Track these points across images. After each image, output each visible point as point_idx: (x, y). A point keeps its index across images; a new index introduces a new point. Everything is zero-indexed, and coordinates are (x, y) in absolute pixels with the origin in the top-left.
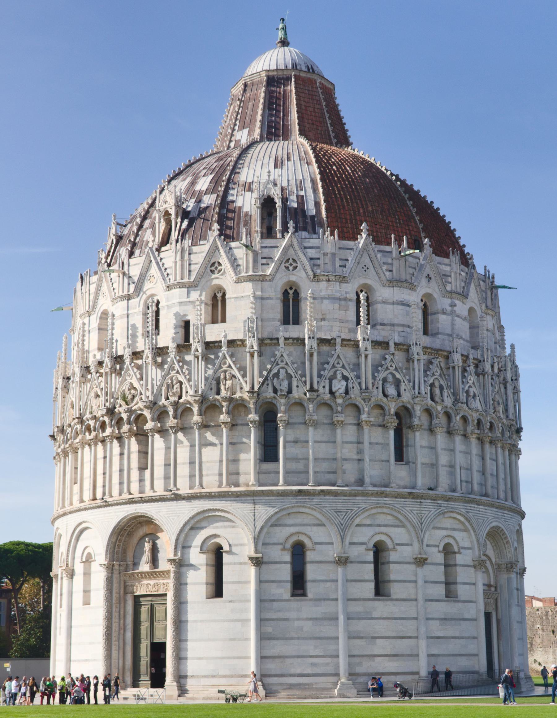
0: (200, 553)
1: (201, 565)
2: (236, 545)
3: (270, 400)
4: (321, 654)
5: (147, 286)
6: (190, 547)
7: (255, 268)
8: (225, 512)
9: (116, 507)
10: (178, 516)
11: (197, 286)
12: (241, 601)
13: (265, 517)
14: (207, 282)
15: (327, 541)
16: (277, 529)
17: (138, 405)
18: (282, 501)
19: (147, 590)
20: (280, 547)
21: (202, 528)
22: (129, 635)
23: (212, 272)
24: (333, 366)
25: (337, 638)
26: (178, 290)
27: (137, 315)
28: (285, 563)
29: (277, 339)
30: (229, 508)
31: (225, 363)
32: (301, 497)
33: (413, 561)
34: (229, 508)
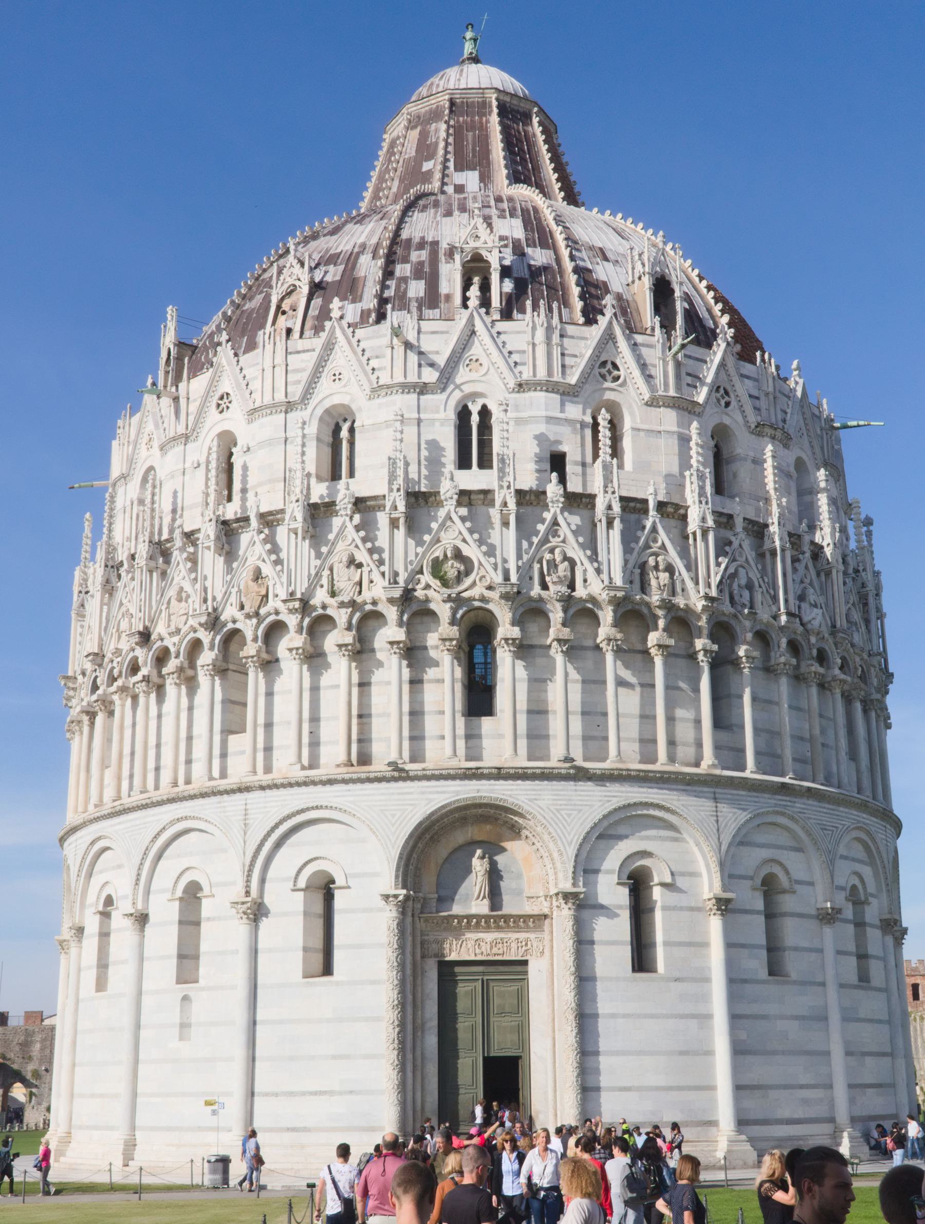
0: (618, 884)
1: (620, 907)
2: (683, 874)
3: (726, 619)
4: (812, 1082)
5: (463, 375)
6: (597, 871)
7: (678, 388)
8: (668, 810)
9: (425, 783)
10: (580, 811)
11: (577, 396)
12: (694, 980)
13: (733, 826)
14: (595, 391)
15: (807, 879)
16: (745, 850)
17: (474, 589)
18: (756, 799)
19: (478, 951)
20: (749, 883)
21: (621, 838)
22: (432, 1041)
23: (603, 377)
24: (802, 582)
25: (828, 1053)
26: (543, 394)
27: (442, 425)
28: (758, 912)
29: (730, 517)
30: (675, 803)
31: (655, 541)
32: (780, 797)
33: (878, 923)
34: (675, 803)
